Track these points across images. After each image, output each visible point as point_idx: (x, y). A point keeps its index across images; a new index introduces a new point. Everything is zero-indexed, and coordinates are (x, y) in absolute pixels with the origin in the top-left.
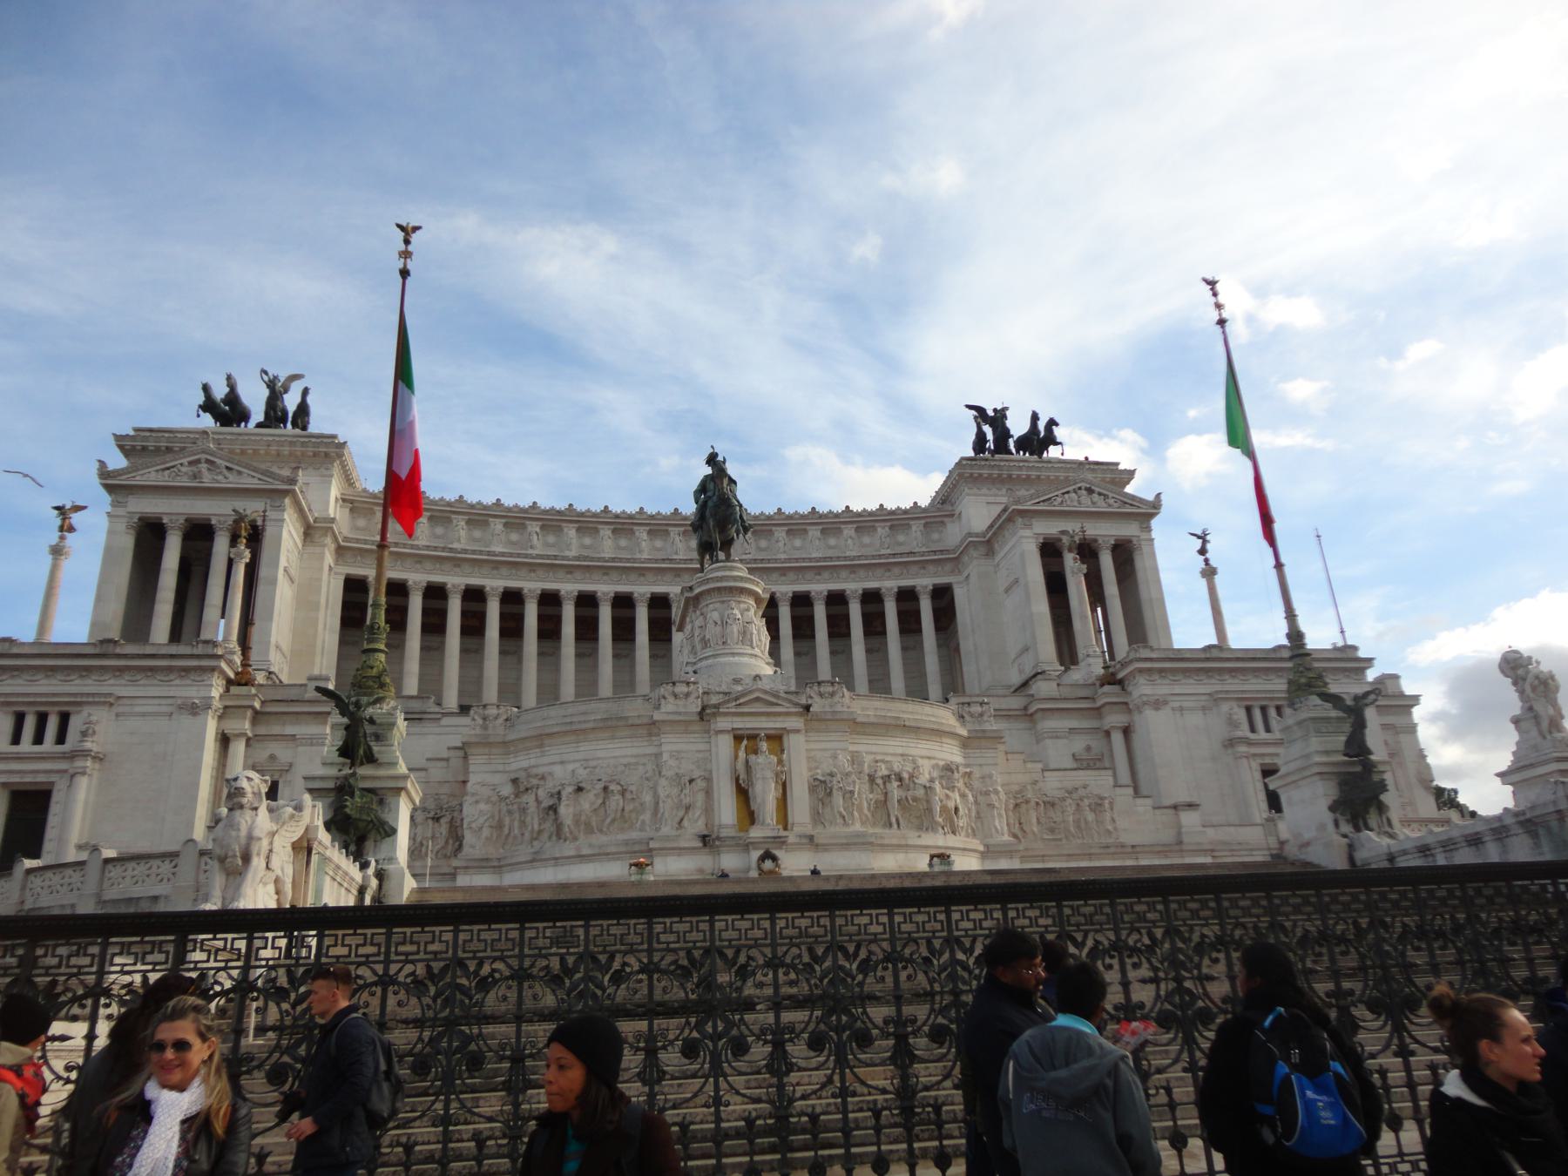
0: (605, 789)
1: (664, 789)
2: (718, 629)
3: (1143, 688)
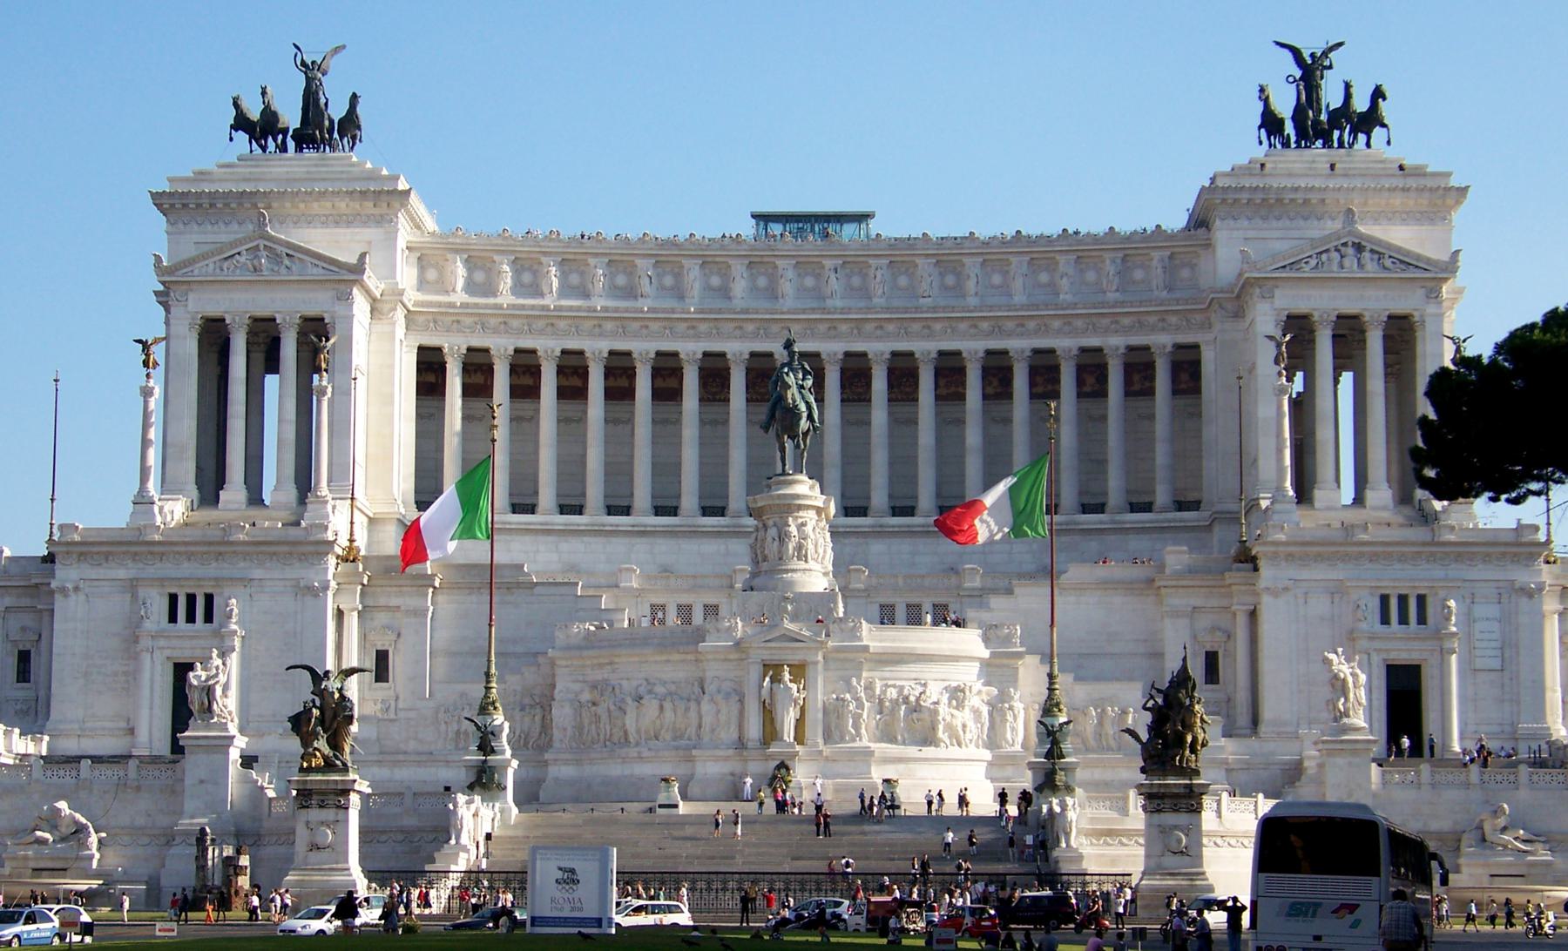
0: (661, 708)
2: (776, 543)
3: (1267, 573)
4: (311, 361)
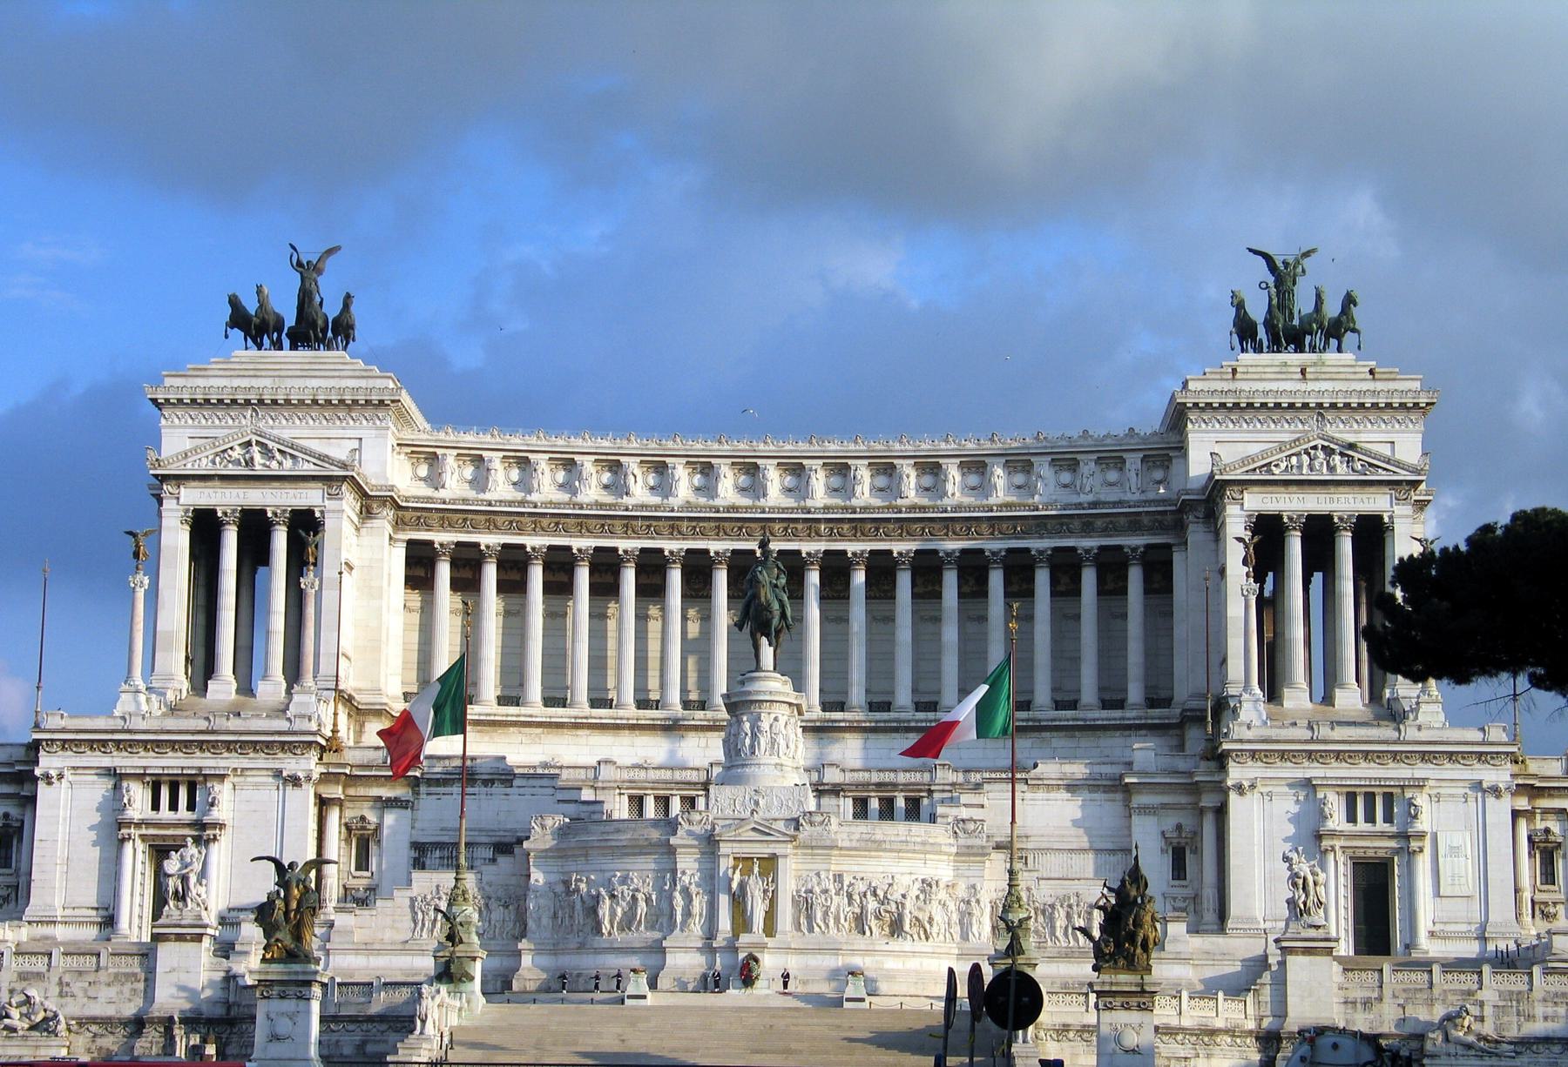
1: (679, 901)
2: (748, 741)
3: (1236, 773)
4: (301, 559)
